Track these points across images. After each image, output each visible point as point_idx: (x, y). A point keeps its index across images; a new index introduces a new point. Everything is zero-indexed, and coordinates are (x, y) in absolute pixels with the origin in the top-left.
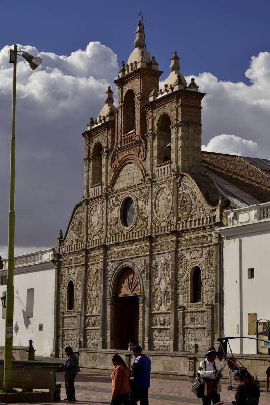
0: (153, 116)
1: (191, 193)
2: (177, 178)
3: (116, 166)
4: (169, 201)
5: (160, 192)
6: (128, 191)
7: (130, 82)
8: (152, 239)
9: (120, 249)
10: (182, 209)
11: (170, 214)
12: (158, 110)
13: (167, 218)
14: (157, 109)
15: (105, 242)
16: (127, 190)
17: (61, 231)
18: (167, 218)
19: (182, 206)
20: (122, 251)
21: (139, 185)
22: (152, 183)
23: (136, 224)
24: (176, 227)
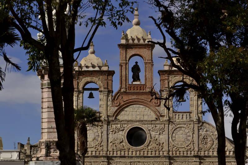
0: (168, 79)
1: (212, 135)
2: (198, 124)
3: (120, 104)
4: (189, 136)
5: (178, 129)
6: (137, 123)
7: (138, 49)
8: (170, 158)
9: (129, 161)
10: (203, 143)
11: (190, 144)
12: (175, 77)
13: (187, 146)
14: (173, 76)
15: (107, 154)
16: (136, 122)
17: (29, 138)
18: (187, 146)
19: (203, 141)
20: (131, 162)
21: (152, 121)
22: (169, 122)
23: (148, 146)
24: (198, 153)
